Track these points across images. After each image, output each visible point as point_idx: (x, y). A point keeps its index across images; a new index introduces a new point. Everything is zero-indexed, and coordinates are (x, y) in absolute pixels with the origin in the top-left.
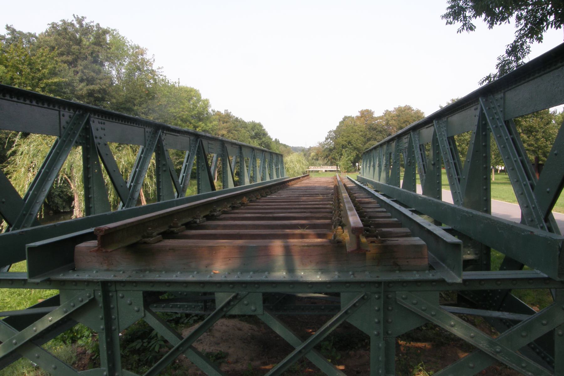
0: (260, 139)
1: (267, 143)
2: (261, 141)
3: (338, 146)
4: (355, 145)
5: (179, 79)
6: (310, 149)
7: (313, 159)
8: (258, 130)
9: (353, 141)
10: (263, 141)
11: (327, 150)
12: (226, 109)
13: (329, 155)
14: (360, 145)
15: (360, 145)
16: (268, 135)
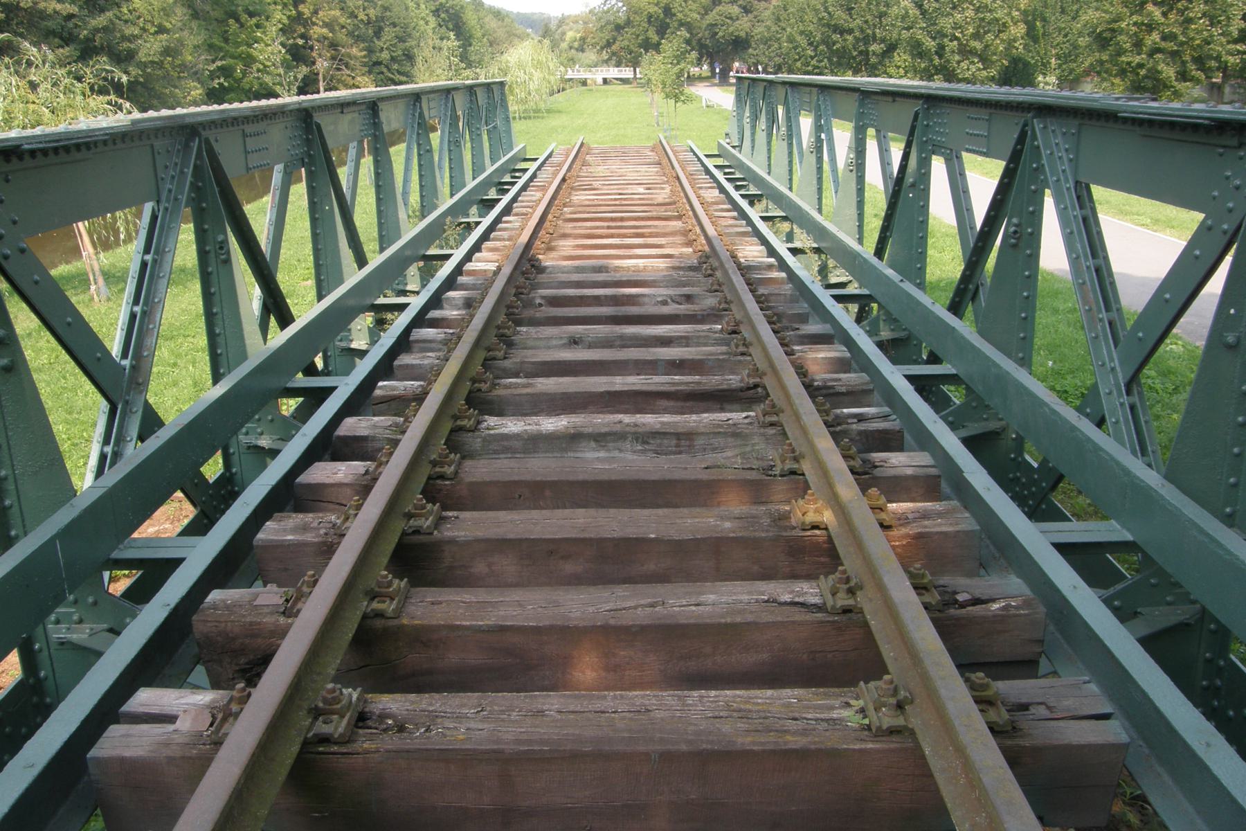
1: (453, 8)
3: (638, 18)
4: (680, 16)
6: (562, 21)
7: (571, 48)
9: (676, 5)
11: (609, 27)
13: (615, 39)
14: (696, 16)
15: (696, 16)
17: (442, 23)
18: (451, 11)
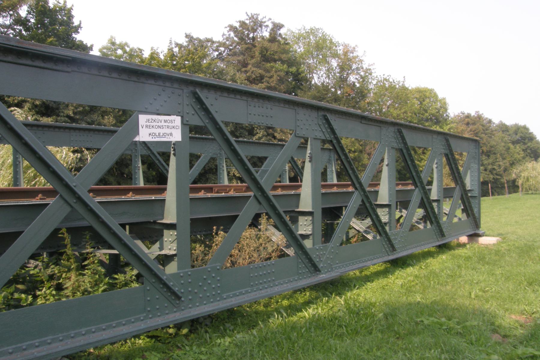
0: (525, 144)
2: (526, 146)
5: (404, 77)
8: (522, 133)
10: (528, 147)
12: (477, 110)
16: (537, 139)
17: (528, 155)
18: (533, 149)
